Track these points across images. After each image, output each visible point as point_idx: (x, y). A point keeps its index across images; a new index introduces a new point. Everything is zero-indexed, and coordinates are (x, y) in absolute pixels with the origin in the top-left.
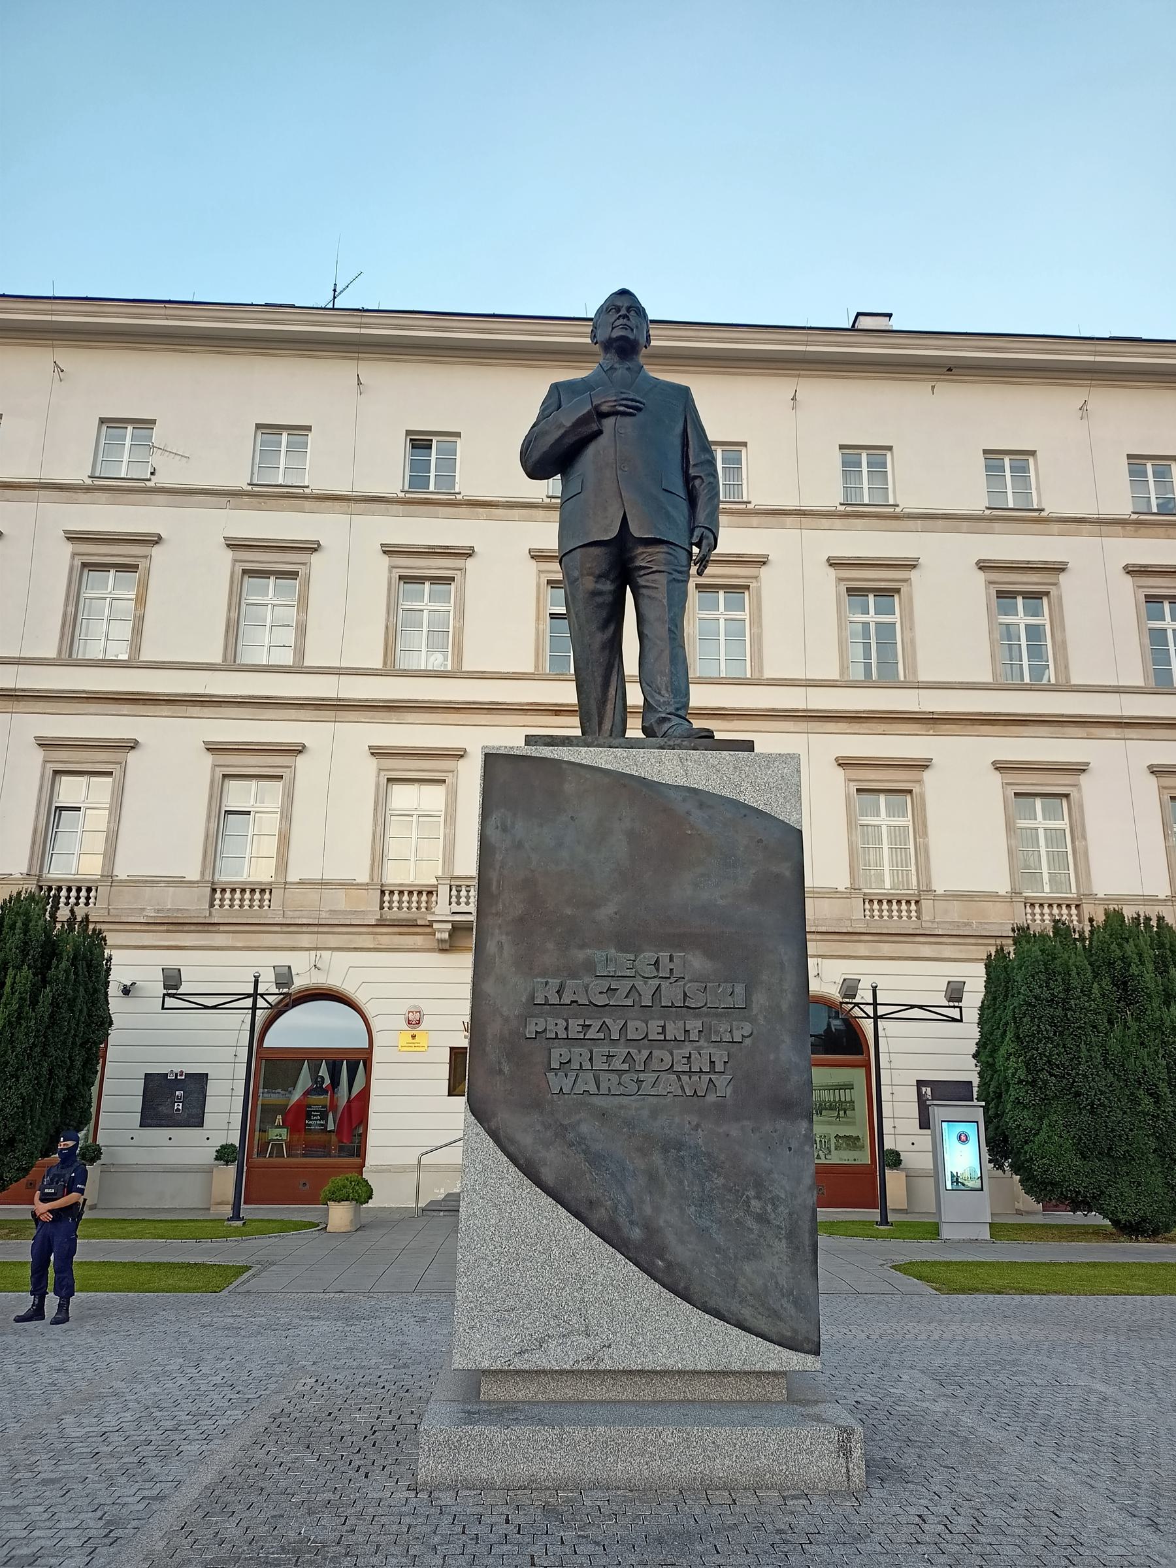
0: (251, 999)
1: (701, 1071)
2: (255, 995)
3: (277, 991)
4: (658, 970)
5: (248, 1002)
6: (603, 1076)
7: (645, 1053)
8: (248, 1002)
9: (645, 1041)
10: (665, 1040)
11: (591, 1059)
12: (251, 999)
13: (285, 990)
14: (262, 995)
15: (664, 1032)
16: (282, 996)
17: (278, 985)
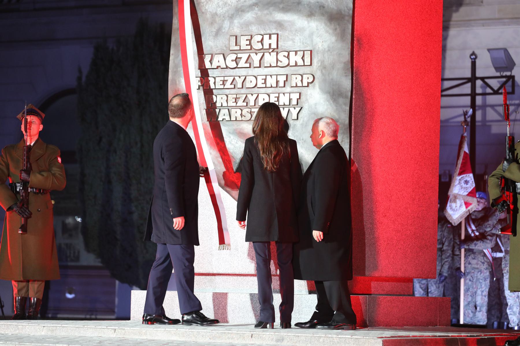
0: (469, 85)
1: (284, 105)
2: (473, 79)
3: (498, 74)
4: (262, 45)
5: (467, 89)
6: (233, 111)
7: (255, 96)
8: (467, 89)
9: (256, 89)
10: (266, 87)
11: (227, 101)
12: (469, 85)
13: (508, 74)
14: (483, 79)
15: (265, 83)
16: (504, 79)
17: (497, 69)
